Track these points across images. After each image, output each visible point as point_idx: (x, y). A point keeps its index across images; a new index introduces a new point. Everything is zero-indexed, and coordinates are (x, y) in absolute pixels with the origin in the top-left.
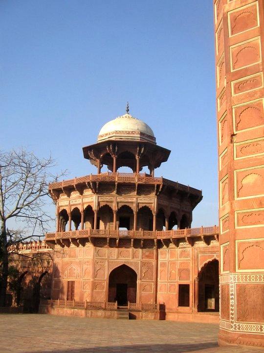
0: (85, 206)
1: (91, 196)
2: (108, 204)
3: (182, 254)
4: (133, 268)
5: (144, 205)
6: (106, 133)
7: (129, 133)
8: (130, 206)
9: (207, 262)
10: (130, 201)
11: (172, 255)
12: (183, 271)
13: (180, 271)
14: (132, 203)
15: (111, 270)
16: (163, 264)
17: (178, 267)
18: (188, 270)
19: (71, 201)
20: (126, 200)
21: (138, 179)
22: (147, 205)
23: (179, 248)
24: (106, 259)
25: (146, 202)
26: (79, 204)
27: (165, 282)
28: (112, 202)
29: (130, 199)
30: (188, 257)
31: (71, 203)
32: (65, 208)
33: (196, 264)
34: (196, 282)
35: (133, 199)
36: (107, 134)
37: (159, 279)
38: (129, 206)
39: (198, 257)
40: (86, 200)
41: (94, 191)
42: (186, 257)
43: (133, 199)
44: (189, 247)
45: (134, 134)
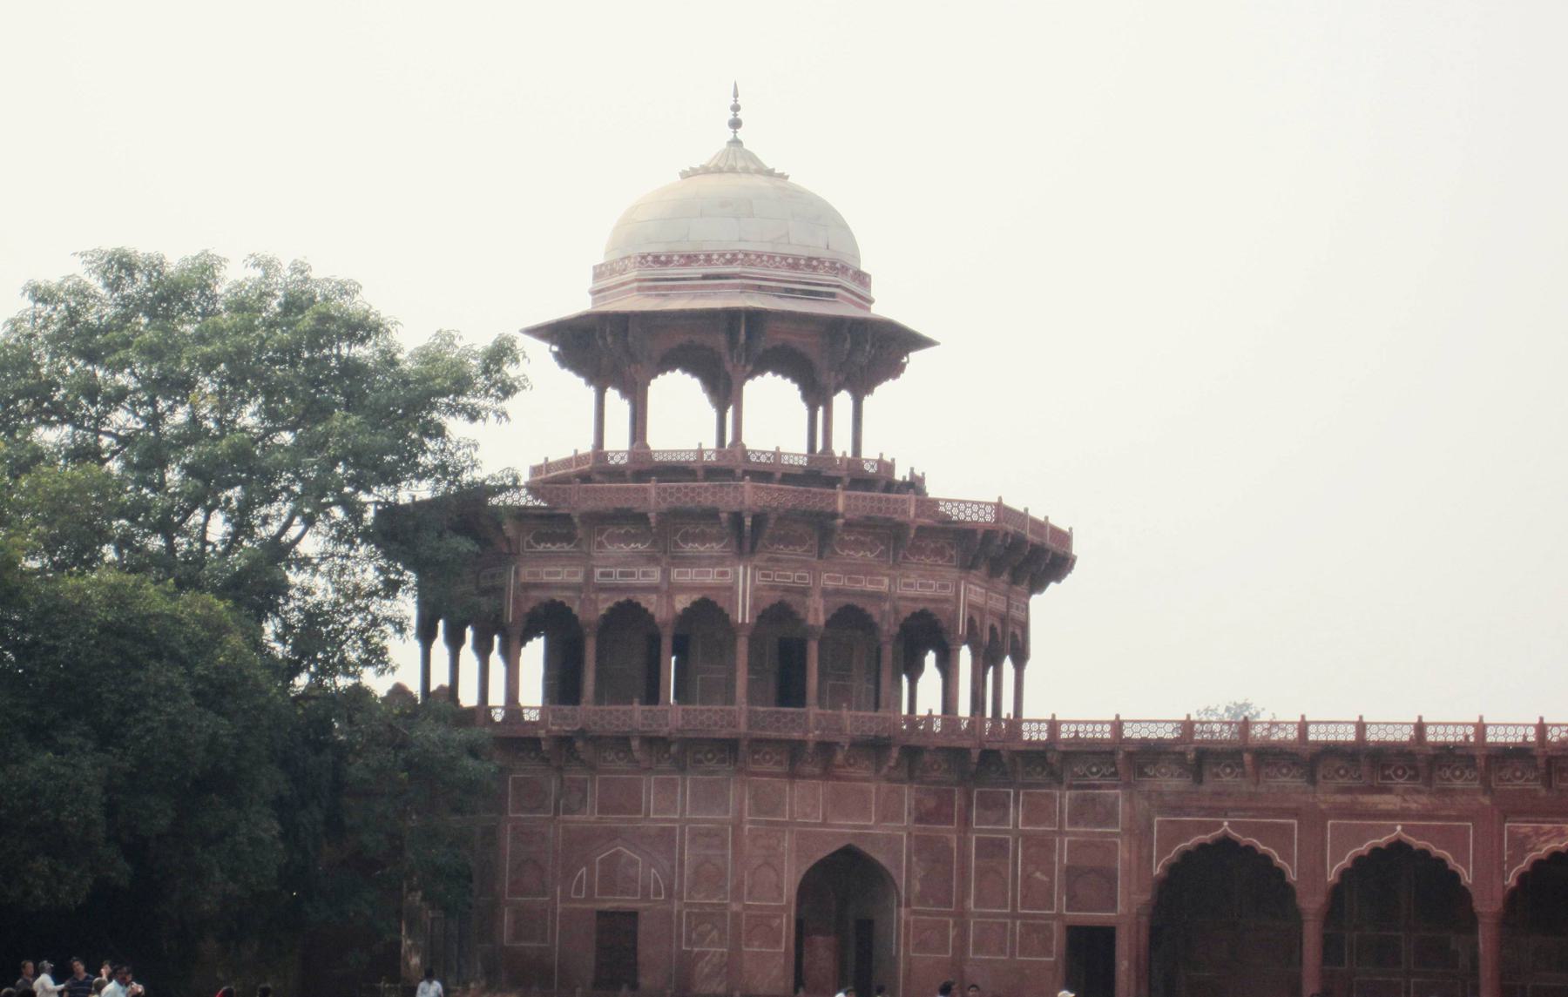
1: (720, 561)
2: (788, 598)
4: (881, 858)
5: (921, 606)
6: (688, 248)
7: (795, 266)
8: (871, 610)
9: (1189, 843)
10: (870, 588)
11: (1036, 812)
12: (1091, 876)
13: (1073, 874)
14: (878, 597)
15: (804, 869)
17: (1062, 857)
18: (1109, 877)
19: (598, 571)
20: (858, 587)
22: (931, 607)
23: (1070, 787)
25: (928, 593)
27: (1006, 916)
28: (804, 592)
29: (871, 582)
30: (1107, 826)
31: (597, 578)
32: (558, 596)
34: (1144, 919)
36: (690, 259)
37: (971, 904)
38: (863, 610)
39: (1151, 826)
43: (880, 583)
44: (1115, 787)
45: (815, 268)
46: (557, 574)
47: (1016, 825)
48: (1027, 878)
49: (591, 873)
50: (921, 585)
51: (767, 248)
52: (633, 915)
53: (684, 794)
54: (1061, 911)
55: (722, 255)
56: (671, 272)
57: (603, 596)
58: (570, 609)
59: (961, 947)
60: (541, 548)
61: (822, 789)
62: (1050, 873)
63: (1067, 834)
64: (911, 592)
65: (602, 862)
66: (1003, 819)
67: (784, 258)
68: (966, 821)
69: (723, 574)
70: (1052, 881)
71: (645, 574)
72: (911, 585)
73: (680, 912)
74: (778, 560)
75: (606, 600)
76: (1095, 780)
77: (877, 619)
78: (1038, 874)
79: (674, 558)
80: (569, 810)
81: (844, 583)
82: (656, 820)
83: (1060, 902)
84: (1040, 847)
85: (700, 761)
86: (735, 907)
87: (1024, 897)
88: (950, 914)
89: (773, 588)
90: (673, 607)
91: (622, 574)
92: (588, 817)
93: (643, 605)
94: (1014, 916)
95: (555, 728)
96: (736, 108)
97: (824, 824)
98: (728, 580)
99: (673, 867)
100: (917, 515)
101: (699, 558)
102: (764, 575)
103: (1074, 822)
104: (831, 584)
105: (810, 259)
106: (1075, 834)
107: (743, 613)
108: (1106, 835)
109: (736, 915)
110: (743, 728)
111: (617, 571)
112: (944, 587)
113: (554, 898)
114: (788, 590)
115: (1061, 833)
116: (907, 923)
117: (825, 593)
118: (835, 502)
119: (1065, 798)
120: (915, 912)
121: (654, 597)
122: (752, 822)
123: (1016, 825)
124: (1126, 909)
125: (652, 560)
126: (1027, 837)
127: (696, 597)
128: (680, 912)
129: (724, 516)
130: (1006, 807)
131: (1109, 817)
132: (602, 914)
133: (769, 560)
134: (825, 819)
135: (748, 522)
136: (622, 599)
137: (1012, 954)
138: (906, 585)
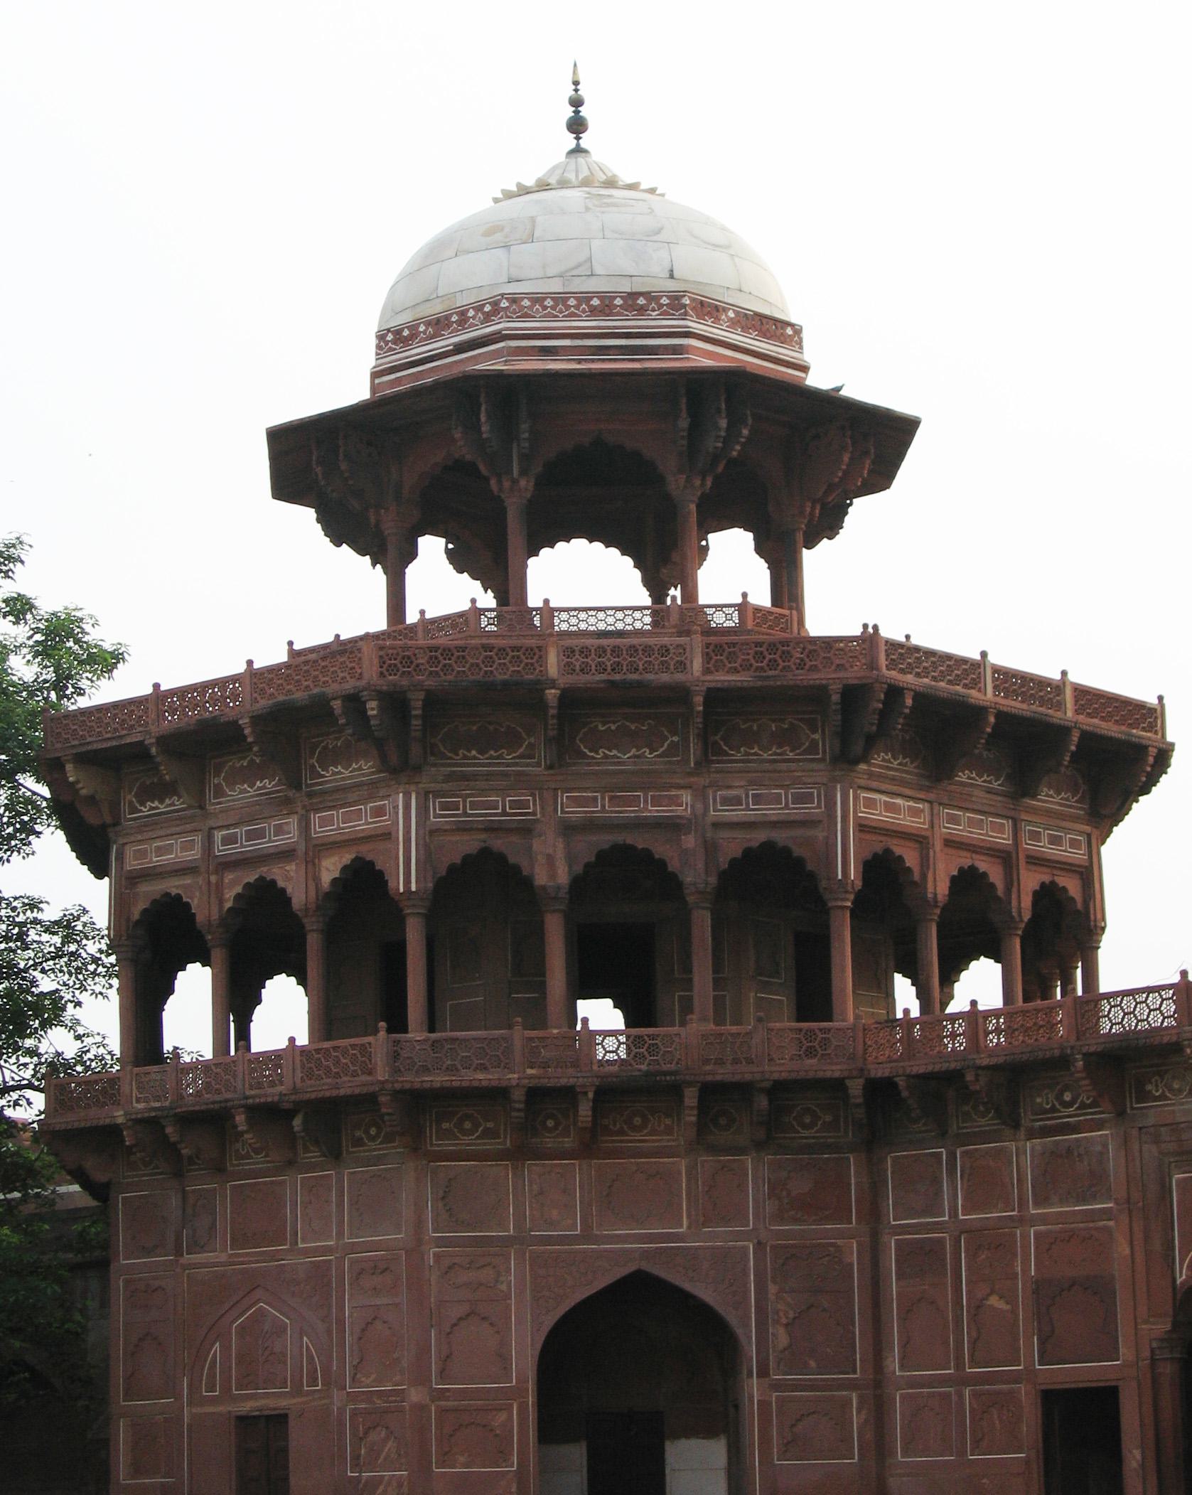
0: (331, 868)
1: (371, 790)
2: (497, 844)
3: (1058, 1176)
5: (760, 836)
6: (435, 309)
8: (662, 849)
10: (653, 811)
11: (986, 1186)
12: (1073, 1298)
13: (1047, 1294)
14: (672, 826)
15: (549, 1321)
16: (922, 1257)
17: (1028, 1266)
18: (1098, 1289)
19: (218, 835)
20: (630, 812)
21: (707, 657)
22: (781, 837)
23: (1031, 1135)
24: (507, 1242)
25: (772, 812)
26: (286, 854)
27: (943, 1381)
28: (526, 830)
30: (1094, 1198)
31: (220, 849)
32: (173, 886)
33: (1157, 1245)
34: (1168, 1370)
35: (675, 801)
36: (439, 324)
37: (893, 1364)
39: (1165, 1191)
40: (332, 824)
41: (394, 759)
42: (1084, 1201)
43: (675, 801)
44: (1099, 1125)
45: (642, 310)
46: (169, 849)
47: (953, 1213)
48: (978, 1307)
49: (226, 1348)
50: (758, 799)
51: (555, 287)
52: (279, 1420)
53: (340, 1204)
54: (1033, 1368)
55: (479, 309)
56: (417, 351)
57: (229, 877)
58: (188, 905)
59: (879, 1447)
60: (145, 811)
61: (579, 1173)
62: (1012, 1300)
63: (1033, 1221)
64: (737, 814)
65: (242, 1327)
66: (932, 1207)
67: (584, 298)
68: (873, 1214)
69: (379, 812)
70: (1014, 1312)
71: (279, 830)
72: (737, 801)
73: (342, 1411)
74: (465, 777)
75: (233, 883)
76: (1069, 1116)
77: (674, 865)
78: (994, 1301)
79: (310, 795)
80: (196, 1246)
81: (603, 807)
82: (306, 1253)
83: (1030, 1345)
84: (992, 1244)
85: (358, 1142)
86: (416, 1395)
87: (974, 1343)
88: (852, 1385)
89: (463, 828)
90: (317, 879)
91: (251, 836)
92: (216, 1257)
93: (281, 884)
94: (962, 1381)
95: (141, 1106)
96: (576, 103)
97: (586, 1237)
98: (385, 821)
99: (329, 1332)
100: (707, 671)
101: (344, 789)
102: (444, 807)
103: (1040, 1201)
104: (576, 812)
105: (634, 295)
106: (1044, 1219)
107: (406, 875)
108: (1090, 1216)
109: (420, 1408)
110: (382, 1074)
111: (241, 831)
112: (807, 798)
113: (178, 1397)
114: (492, 828)
115: (1022, 1221)
116: (764, 1404)
117: (569, 829)
118: (542, 659)
119: (1024, 1155)
120: (777, 1386)
121: (291, 867)
122: (440, 1242)
123: (953, 1213)
124: (1131, 1355)
125: (284, 804)
126: (972, 1231)
127: (347, 858)
128: (342, 1411)
129: (337, 705)
130: (936, 1181)
131: (1094, 1184)
132: (243, 1420)
133: (450, 778)
134: (586, 1226)
135: (372, 708)
136: (252, 878)
137: (962, 1453)
138: (726, 801)
